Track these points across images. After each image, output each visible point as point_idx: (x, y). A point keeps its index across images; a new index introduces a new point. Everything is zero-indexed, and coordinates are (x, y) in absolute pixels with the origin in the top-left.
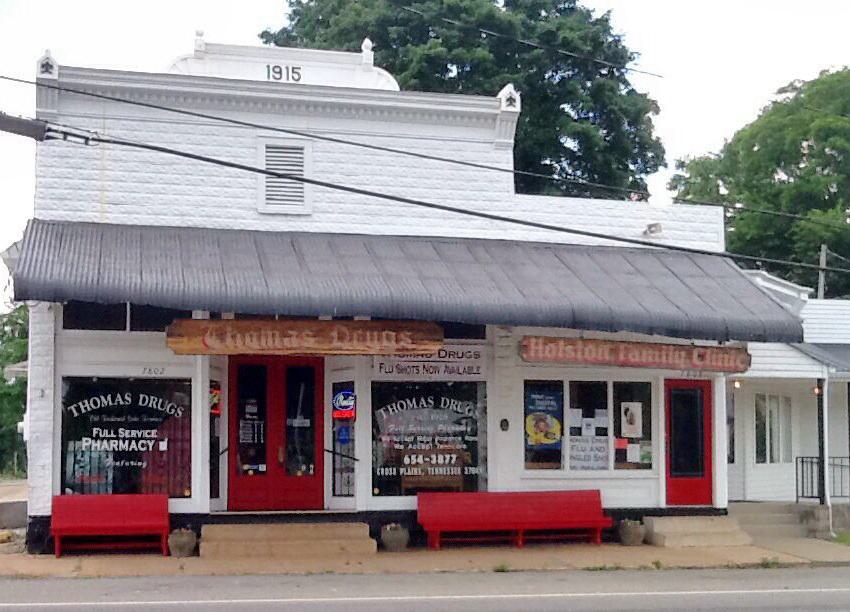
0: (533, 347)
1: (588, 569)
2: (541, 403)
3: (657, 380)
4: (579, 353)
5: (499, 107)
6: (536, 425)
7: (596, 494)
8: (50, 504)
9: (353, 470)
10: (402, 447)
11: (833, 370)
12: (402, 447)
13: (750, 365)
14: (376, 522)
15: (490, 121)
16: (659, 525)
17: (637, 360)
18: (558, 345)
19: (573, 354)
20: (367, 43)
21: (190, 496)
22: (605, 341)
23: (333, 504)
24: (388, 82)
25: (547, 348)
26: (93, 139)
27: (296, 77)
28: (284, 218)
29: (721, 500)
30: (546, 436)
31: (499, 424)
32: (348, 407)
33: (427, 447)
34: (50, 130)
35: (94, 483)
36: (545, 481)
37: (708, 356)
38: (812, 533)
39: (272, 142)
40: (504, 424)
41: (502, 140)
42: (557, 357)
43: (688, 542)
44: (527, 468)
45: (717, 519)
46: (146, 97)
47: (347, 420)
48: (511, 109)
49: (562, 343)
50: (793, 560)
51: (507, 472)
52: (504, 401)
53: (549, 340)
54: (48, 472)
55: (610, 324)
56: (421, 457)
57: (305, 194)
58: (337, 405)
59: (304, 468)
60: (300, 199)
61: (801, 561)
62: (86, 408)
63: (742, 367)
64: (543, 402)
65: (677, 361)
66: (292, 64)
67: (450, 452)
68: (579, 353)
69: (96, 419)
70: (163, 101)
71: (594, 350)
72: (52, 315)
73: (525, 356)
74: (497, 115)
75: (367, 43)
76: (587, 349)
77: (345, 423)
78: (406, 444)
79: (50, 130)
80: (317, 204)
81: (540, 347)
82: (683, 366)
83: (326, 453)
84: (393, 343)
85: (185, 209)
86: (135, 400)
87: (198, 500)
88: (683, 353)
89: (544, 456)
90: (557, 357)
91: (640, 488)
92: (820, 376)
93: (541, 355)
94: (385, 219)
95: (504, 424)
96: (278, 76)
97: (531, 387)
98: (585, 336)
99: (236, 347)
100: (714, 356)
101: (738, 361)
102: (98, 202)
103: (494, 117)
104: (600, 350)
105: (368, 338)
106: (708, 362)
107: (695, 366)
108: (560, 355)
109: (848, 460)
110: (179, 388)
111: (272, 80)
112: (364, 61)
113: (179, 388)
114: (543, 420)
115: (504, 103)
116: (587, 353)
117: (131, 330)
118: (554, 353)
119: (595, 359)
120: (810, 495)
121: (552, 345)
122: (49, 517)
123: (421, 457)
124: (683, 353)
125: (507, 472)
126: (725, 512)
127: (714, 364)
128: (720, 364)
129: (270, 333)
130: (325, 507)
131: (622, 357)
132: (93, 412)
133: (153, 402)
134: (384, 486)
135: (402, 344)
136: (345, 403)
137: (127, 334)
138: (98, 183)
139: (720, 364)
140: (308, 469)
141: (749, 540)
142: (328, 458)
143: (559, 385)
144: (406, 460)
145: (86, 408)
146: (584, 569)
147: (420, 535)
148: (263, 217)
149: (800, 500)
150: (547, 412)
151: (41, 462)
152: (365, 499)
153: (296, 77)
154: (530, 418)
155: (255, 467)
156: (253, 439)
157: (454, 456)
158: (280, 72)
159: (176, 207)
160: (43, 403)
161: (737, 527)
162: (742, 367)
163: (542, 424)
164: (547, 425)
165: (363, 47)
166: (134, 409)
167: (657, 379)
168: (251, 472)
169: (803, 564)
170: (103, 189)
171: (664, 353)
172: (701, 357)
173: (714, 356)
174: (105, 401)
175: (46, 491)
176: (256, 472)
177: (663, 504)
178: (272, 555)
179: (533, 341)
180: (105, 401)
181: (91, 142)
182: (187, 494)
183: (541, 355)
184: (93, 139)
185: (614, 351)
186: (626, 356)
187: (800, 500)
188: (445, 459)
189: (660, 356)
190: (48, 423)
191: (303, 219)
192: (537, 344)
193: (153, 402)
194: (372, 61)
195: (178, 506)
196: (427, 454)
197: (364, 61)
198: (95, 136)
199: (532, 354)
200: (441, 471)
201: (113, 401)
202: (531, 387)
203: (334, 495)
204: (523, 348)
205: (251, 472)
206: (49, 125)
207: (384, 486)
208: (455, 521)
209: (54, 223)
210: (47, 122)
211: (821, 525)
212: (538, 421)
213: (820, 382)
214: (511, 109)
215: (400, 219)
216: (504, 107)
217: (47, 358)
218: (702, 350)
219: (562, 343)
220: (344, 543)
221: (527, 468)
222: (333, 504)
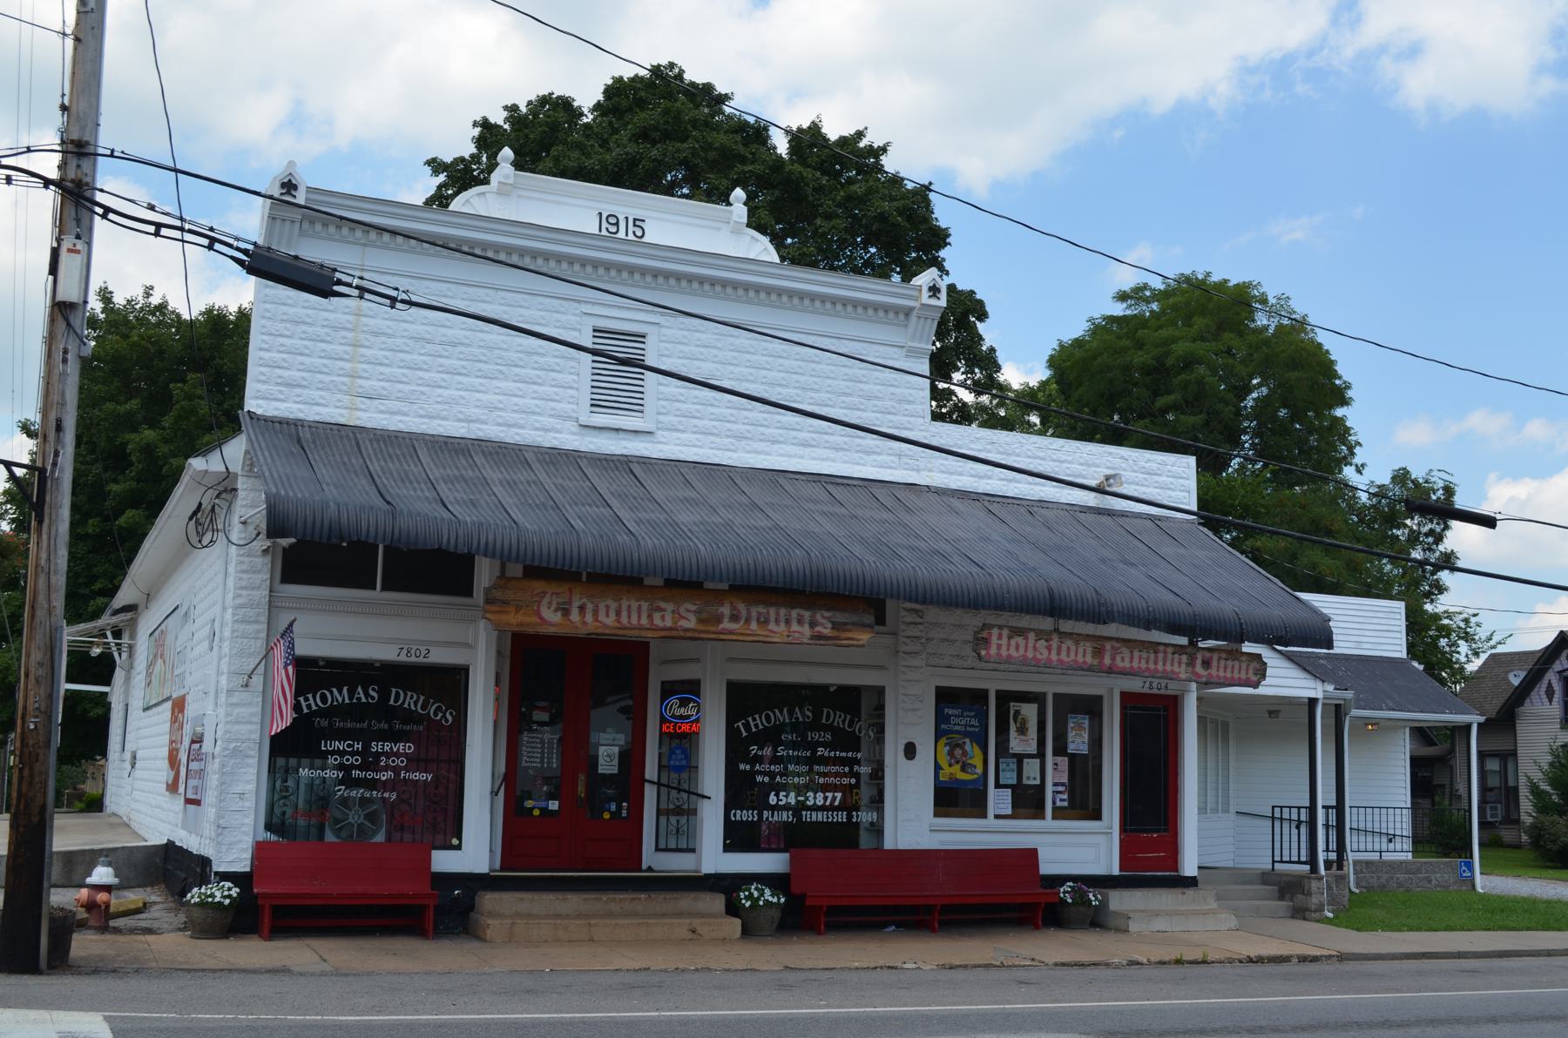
0: (994, 640)
1: (1064, 964)
2: (957, 720)
3: (1111, 691)
4: (1054, 652)
5: (917, 299)
6: (951, 754)
7: (1033, 853)
8: (248, 855)
9: (694, 812)
10: (767, 779)
11: (1330, 688)
12: (767, 779)
13: (1264, 676)
14: (728, 885)
15: (902, 317)
16: (1120, 901)
17: (1127, 664)
18: (1026, 638)
19: (1046, 652)
20: (739, 194)
21: (459, 847)
22: (1089, 637)
23: (652, 859)
24: (761, 248)
25: (1013, 642)
26: (403, 301)
27: (639, 233)
28: (613, 435)
29: (1189, 868)
30: (963, 769)
31: (901, 754)
32: (688, 717)
33: (802, 780)
34: (339, 282)
35: (301, 822)
36: (964, 834)
37: (1215, 663)
38: (1300, 913)
39: (602, 324)
40: (910, 751)
41: (916, 345)
42: (1025, 657)
43: (1160, 924)
44: (936, 815)
45: (1190, 892)
46: (540, 262)
47: (684, 736)
48: (933, 302)
49: (1032, 636)
50: (1317, 952)
51: (911, 821)
52: (910, 720)
53: (1017, 632)
54: (249, 804)
55: (1098, 613)
56: (792, 794)
57: (590, 390)
58: (667, 715)
59: (613, 807)
60: (638, 408)
61: (1326, 953)
62: (309, 706)
63: (1254, 678)
64: (961, 720)
65: (1176, 669)
66: (633, 213)
67: (834, 788)
68: (1054, 652)
69: (325, 723)
70: (564, 269)
71: (1073, 648)
72: (268, 559)
73: (983, 653)
74: (911, 309)
75: (739, 194)
76: (1064, 647)
77: (682, 744)
78: (772, 775)
79: (339, 282)
80: (661, 418)
81: (1004, 641)
82: (1183, 676)
83: (647, 785)
84: (807, 626)
85: (475, 412)
86: (384, 695)
87: (475, 849)
88: (1184, 658)
89: (955, 799)
90: (1025, 657)
91: (1081, 849)
92: (1312, 694)
93: (1004, 652)
94: (820, 452)
95: (910, 751)
96: (613, 229)
97: (946, 697)
98: (1062, 629)
99: (585, 623)
100: (1222, 663)
101: (1251, 672)
102: (346, 393)
103: (908, 312)
104: (1081, 650)
105: (772, 618)
106: (1214, 672)
107: (1197, 675)
108: (1030, 654)
109: (1407, 814)
110: (448, 684)
111: (604, 233)
112: (735, 218)
113: (448, 684)
114: (962, 746)
115: (925, 294)
116: (1064, 653)
117: (384, 589)
118: (1022, 651)
119: (1075, 661)
120: (1286, 858)
121: (1020, 640)
122: (857, 846)
123: (792, 794)
124: (1184, 658)
125: (911, 821)
126: (1191, 882)
127: (1222, 674)
128: (1229, 675)
129: (614, 605)
130: (644, 867)
131: (1107, 661)
132: (320, 713)
133: (409, 700)
134: (738, 838)
135: (818, 628)
136: (682, 711)
137: (377, 594)
138: (347, 365)
139: (1143, 665)
140: (619, 808)
141: (1233, 922)
142: (650, 793)
143: (982, 695)
144: (772, 800)
145: (309, 706)
146: (1056, 964)
147: (803, 913)
148: (587, 431)
149: (1277, 866)
150: (966, 734)
151: (238, 789)
152: (713, 857)
153: (639, 233)
154: (943, 741)
155: (543, 804)
156: (542, 762)
157: (839, 795)
158: (617, 224)
159: (459, 408)
160: (244, 696)
161: (1213, 905)
162: (1254, 678)
163: (958, 752)
164: (965, 753)
165: (732, 199)
166: (383, 710)
167: (1111, 690)
168: (536, 812)
169: (1330, 956)
170: (354, 376)
171: (1161, 656)
172: (1207, 664)
173: (1222, 663)
174: (340, 696)
175: (244, 833)
176: (544, 811)
177: (1116, 872)
178: (592, 940)
179: (995, 632)
180: (340, 696)
181: (399, 305)
182: (455, 842)
183: (1004, 652)
184: (403, 301)
185: (1099, 652)
186: (1113, 659)
187: (1277, 866)
188: (826, 798)
189: (1156, 663)
190: (253, 727)
191: (642, 437)
192: (1000, 637)
193: (409, 700)
194: (745, 220)
195: (444, 861)
196: (800, 790)
197: (735, 218)
198: (404, 297)
199: (993, 651)
200: (819, 817)
201: (351, 698)
202: (946, 697)
203: (657, 849)
204: (980, 641)
205: (536, 812)
206: (338, 275)
207: (738, 838)
208: (839, 892)
209: (282, 422)
210: (335, 270)
211: (1315, 900)
212: (953, 746)
213: (1312, 702)
214: (933, 302)
215: (776, 446)
216: (925, 298)
217: (256, 627)
218: (1208, 655)
219: (1032, 636)
220: (696, 922)
221: (936, 815)
222: (652, 859)
